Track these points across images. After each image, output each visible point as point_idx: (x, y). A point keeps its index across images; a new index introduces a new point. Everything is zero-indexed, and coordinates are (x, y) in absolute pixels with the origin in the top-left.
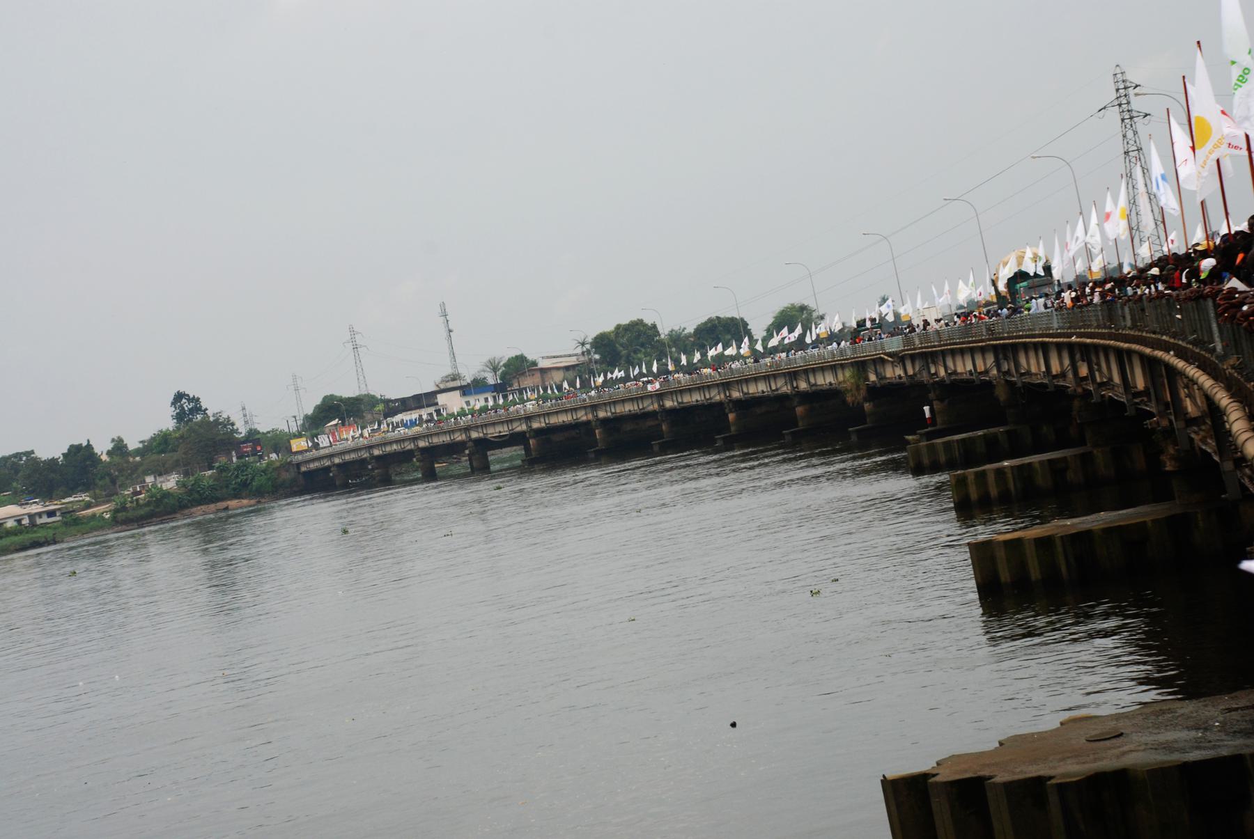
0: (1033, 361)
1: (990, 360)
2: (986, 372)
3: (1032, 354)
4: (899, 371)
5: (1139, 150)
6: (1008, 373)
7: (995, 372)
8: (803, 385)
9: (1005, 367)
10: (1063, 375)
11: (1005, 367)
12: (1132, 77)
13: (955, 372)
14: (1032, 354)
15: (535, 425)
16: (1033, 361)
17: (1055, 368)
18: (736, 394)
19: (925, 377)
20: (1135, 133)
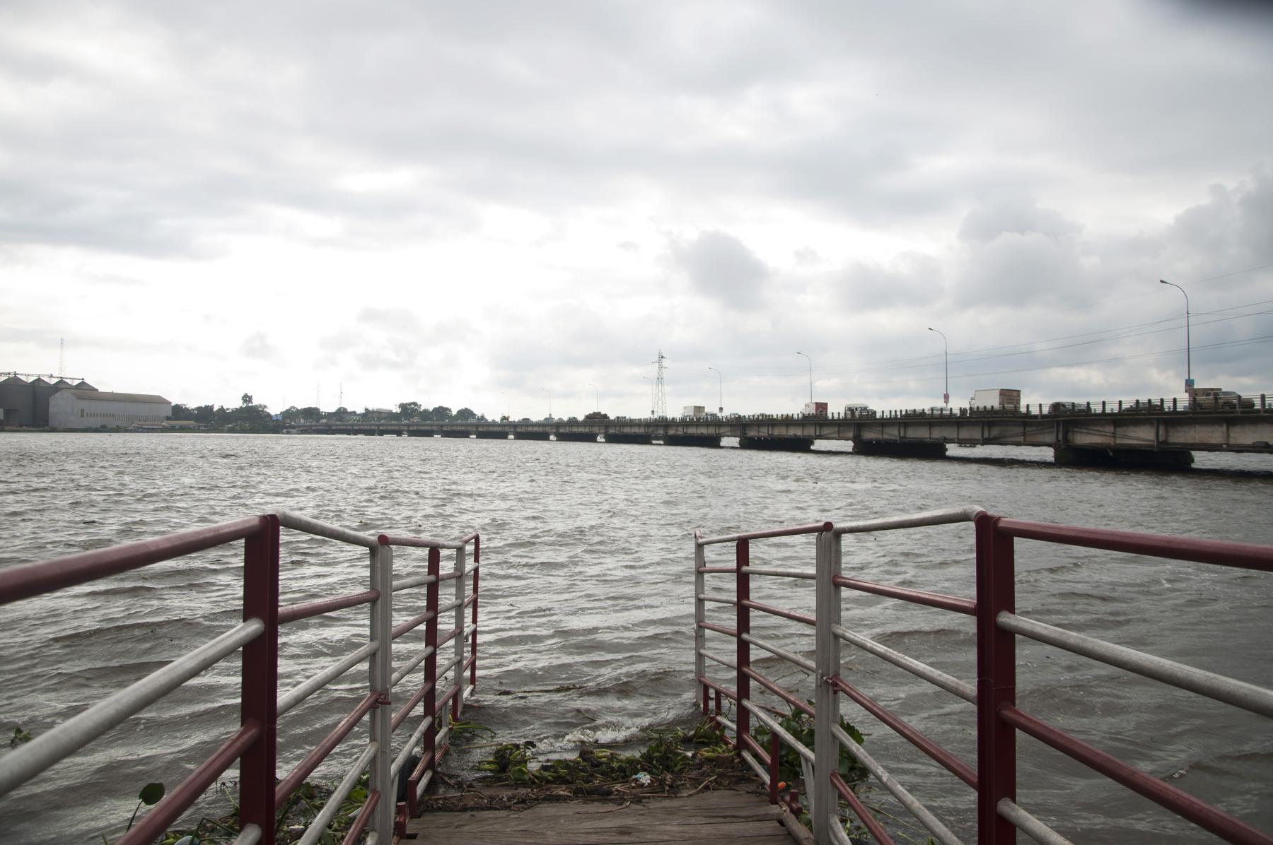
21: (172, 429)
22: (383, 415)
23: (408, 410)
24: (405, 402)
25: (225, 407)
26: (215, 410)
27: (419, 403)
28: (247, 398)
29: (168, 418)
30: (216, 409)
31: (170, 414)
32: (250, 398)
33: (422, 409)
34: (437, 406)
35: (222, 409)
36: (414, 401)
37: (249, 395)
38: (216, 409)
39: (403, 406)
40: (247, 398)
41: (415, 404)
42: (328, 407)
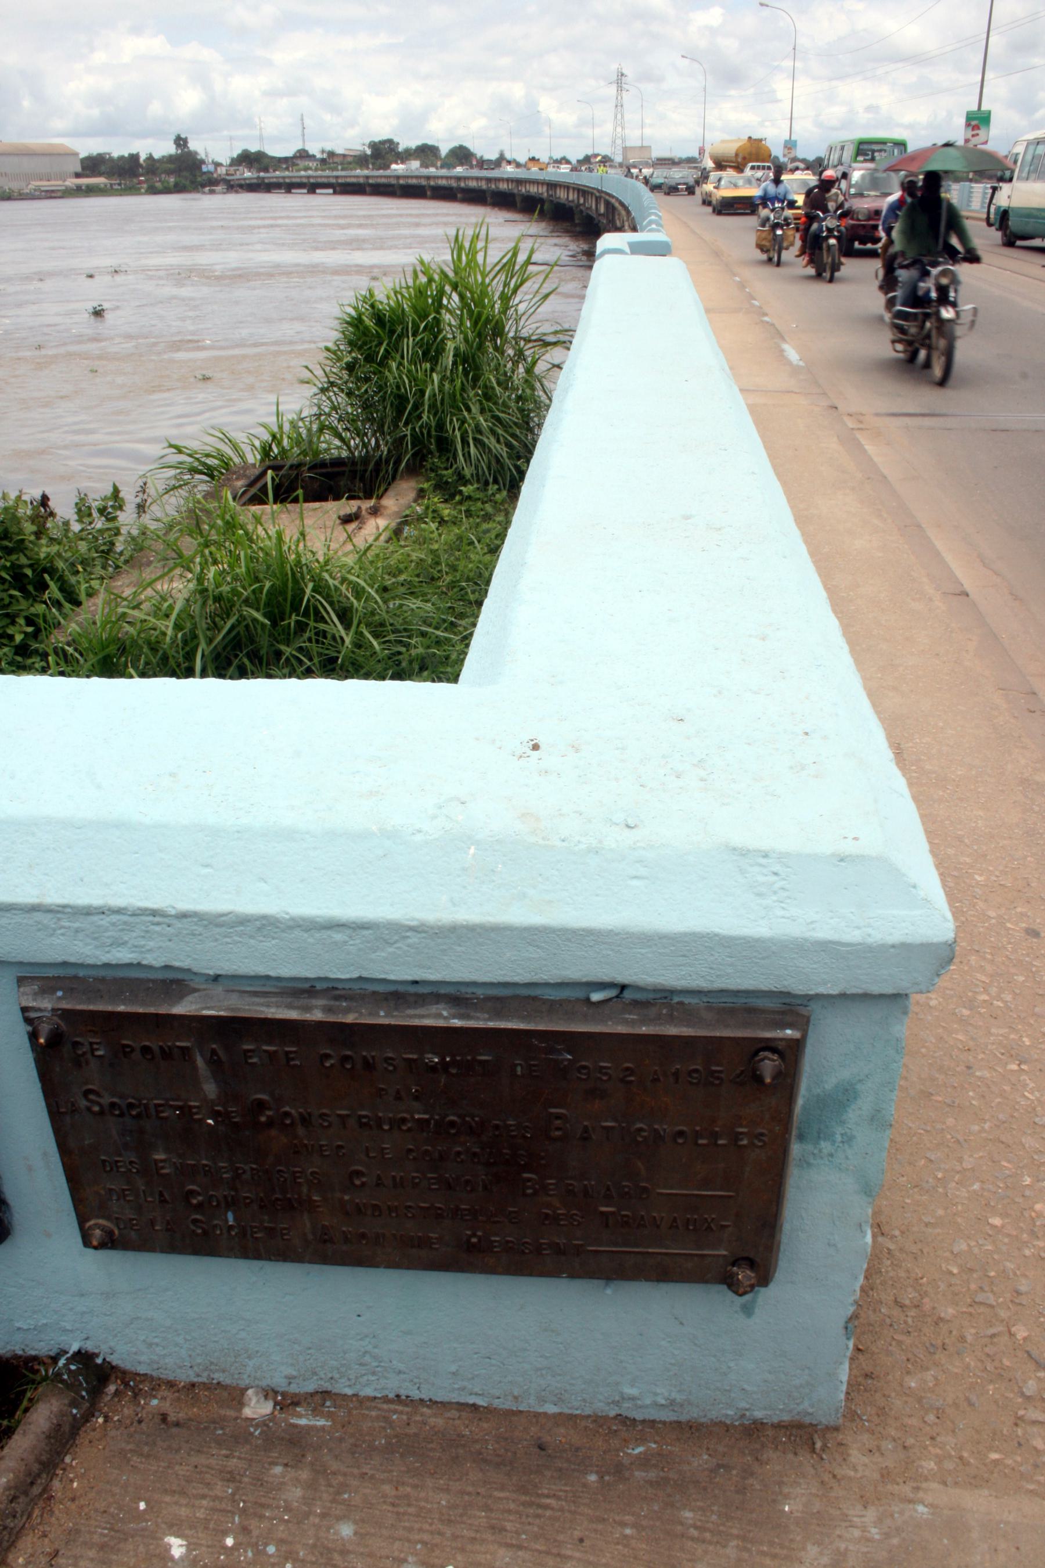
4: (505, 186)
8: (462, 185)
15: (340, 181)
17: (571, 198)
18: (432, 183)
19: (516, 191)
21: (80, 192)
22: (350, 159)
24: (377, 140)
25: (156, 156)
26: (142, 160)
27: (396, 140)
28: (181, 142)
29: (78, 175)
30: (143, 157)
31: (79, 169)
32: (185, 141)
33: (401, 149)
35: (150, 158)
37: (183, 136)
38: (143, 157)
39: (374, 146)
40: (181, 142)
41: (390, 141)
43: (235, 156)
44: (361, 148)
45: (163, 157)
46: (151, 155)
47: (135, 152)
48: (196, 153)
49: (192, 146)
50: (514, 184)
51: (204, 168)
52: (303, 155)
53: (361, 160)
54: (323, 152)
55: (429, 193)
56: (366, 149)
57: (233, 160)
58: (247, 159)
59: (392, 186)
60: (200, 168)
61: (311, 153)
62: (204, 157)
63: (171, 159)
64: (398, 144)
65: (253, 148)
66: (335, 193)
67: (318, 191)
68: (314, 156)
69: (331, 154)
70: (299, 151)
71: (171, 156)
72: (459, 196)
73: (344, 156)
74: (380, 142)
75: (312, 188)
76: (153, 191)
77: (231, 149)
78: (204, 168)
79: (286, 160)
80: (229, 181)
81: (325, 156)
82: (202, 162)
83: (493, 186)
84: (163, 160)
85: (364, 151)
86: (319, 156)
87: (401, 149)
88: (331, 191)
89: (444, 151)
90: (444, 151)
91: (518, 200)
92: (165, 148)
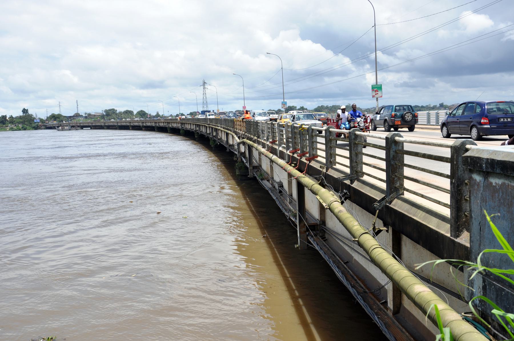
0: (188, 126)
1: (180, 124)
2: (179, 127)
3: (188, 125)
4: (163, 124)
5: (205, 94)
6: (183, 127)
7: (180, 127)
8: (144, 125)
9: (182, 126)
10: (193, 129)
11: (182, 126)
12: (205, 82)
13: (173, 126)
14: (188, 125)
16: (188, 126)
18: (132, 124)
19: (167, 126)
20: (205, 91)
23: (110, 113)
24: (108, 109)
25: (14, 116)
26: (7, 118)
27: (115, 109)
28: (25, 111)
33: (118, 112)
34: (125, 110)
35: (11, 117)
36: (113, 108)
37: (26, 109)
39: (106, 111)
40: (25, 111)
41: (113, 109)
42: (67, 111)
43: (49, 116)
44: (102, 112)
45: (17, 117)
46: (11, 116)
47: (4, 115)
48: (32, 115)
49: (30, 112)
50: (166, 124)
51: (35, 121)
52: (77, 115)
53: (103, 116)
54: (86, 114)
55: (130, 128)
56: (104, 112)
57: (47, 118)
58: (54, 117)
59: (115, 126)
60: (33, 120)
61: (81, 114)
62: (35, 116)
63: (20, 117)
64: (117, 110)
65: (56, 112)
66: (91, 129)
67: (84, 128)
68: (82, 116)
69: (90, 115)
70: (76, 114)
71: (21, 116)
72: (143, 129)
73: (95, 115)
74: (109, 110)
75: (82, 127)
76: (12, 129)
77: (47, 114)
78: (35, 121)
79: (70, 117)
80: (46, 125)
81: (87, 115)
82: (35, 118)
83: (157, 125)
84: (16, 118)
85: (103, 113)
86: (84, 115)
87: (118, 112)
88: (90, 128)
89: (135, 112)
90: (135, 112)
91: (168, 129)
92: (17, 113)
